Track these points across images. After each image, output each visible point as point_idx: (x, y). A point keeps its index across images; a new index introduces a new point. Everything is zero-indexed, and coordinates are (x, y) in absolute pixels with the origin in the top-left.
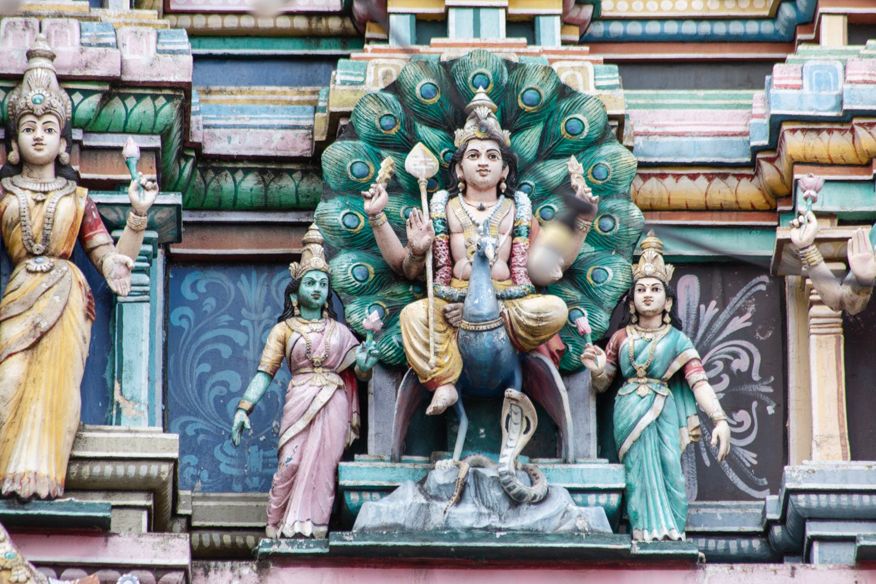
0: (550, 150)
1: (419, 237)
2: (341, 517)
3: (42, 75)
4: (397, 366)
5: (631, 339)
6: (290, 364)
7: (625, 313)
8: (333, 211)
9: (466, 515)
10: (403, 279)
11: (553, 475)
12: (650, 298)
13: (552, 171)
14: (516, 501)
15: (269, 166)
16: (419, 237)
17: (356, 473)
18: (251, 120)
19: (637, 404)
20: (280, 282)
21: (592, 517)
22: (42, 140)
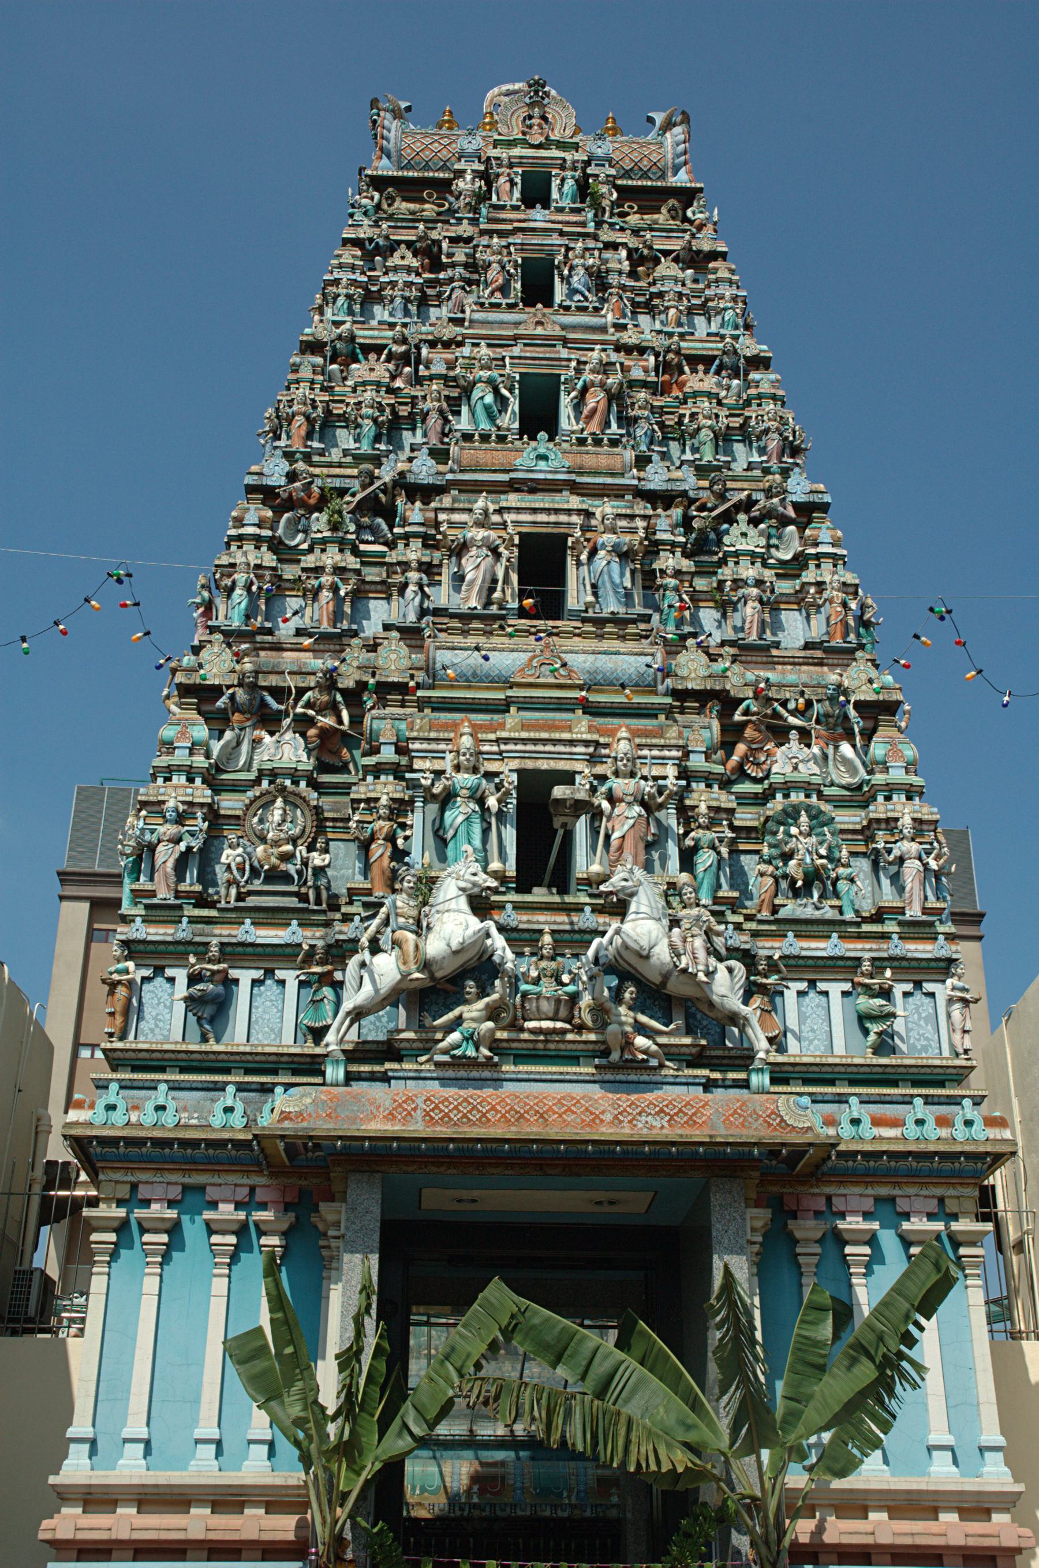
10: (787, 857)
11: (828, 903)
18: (746, 817)
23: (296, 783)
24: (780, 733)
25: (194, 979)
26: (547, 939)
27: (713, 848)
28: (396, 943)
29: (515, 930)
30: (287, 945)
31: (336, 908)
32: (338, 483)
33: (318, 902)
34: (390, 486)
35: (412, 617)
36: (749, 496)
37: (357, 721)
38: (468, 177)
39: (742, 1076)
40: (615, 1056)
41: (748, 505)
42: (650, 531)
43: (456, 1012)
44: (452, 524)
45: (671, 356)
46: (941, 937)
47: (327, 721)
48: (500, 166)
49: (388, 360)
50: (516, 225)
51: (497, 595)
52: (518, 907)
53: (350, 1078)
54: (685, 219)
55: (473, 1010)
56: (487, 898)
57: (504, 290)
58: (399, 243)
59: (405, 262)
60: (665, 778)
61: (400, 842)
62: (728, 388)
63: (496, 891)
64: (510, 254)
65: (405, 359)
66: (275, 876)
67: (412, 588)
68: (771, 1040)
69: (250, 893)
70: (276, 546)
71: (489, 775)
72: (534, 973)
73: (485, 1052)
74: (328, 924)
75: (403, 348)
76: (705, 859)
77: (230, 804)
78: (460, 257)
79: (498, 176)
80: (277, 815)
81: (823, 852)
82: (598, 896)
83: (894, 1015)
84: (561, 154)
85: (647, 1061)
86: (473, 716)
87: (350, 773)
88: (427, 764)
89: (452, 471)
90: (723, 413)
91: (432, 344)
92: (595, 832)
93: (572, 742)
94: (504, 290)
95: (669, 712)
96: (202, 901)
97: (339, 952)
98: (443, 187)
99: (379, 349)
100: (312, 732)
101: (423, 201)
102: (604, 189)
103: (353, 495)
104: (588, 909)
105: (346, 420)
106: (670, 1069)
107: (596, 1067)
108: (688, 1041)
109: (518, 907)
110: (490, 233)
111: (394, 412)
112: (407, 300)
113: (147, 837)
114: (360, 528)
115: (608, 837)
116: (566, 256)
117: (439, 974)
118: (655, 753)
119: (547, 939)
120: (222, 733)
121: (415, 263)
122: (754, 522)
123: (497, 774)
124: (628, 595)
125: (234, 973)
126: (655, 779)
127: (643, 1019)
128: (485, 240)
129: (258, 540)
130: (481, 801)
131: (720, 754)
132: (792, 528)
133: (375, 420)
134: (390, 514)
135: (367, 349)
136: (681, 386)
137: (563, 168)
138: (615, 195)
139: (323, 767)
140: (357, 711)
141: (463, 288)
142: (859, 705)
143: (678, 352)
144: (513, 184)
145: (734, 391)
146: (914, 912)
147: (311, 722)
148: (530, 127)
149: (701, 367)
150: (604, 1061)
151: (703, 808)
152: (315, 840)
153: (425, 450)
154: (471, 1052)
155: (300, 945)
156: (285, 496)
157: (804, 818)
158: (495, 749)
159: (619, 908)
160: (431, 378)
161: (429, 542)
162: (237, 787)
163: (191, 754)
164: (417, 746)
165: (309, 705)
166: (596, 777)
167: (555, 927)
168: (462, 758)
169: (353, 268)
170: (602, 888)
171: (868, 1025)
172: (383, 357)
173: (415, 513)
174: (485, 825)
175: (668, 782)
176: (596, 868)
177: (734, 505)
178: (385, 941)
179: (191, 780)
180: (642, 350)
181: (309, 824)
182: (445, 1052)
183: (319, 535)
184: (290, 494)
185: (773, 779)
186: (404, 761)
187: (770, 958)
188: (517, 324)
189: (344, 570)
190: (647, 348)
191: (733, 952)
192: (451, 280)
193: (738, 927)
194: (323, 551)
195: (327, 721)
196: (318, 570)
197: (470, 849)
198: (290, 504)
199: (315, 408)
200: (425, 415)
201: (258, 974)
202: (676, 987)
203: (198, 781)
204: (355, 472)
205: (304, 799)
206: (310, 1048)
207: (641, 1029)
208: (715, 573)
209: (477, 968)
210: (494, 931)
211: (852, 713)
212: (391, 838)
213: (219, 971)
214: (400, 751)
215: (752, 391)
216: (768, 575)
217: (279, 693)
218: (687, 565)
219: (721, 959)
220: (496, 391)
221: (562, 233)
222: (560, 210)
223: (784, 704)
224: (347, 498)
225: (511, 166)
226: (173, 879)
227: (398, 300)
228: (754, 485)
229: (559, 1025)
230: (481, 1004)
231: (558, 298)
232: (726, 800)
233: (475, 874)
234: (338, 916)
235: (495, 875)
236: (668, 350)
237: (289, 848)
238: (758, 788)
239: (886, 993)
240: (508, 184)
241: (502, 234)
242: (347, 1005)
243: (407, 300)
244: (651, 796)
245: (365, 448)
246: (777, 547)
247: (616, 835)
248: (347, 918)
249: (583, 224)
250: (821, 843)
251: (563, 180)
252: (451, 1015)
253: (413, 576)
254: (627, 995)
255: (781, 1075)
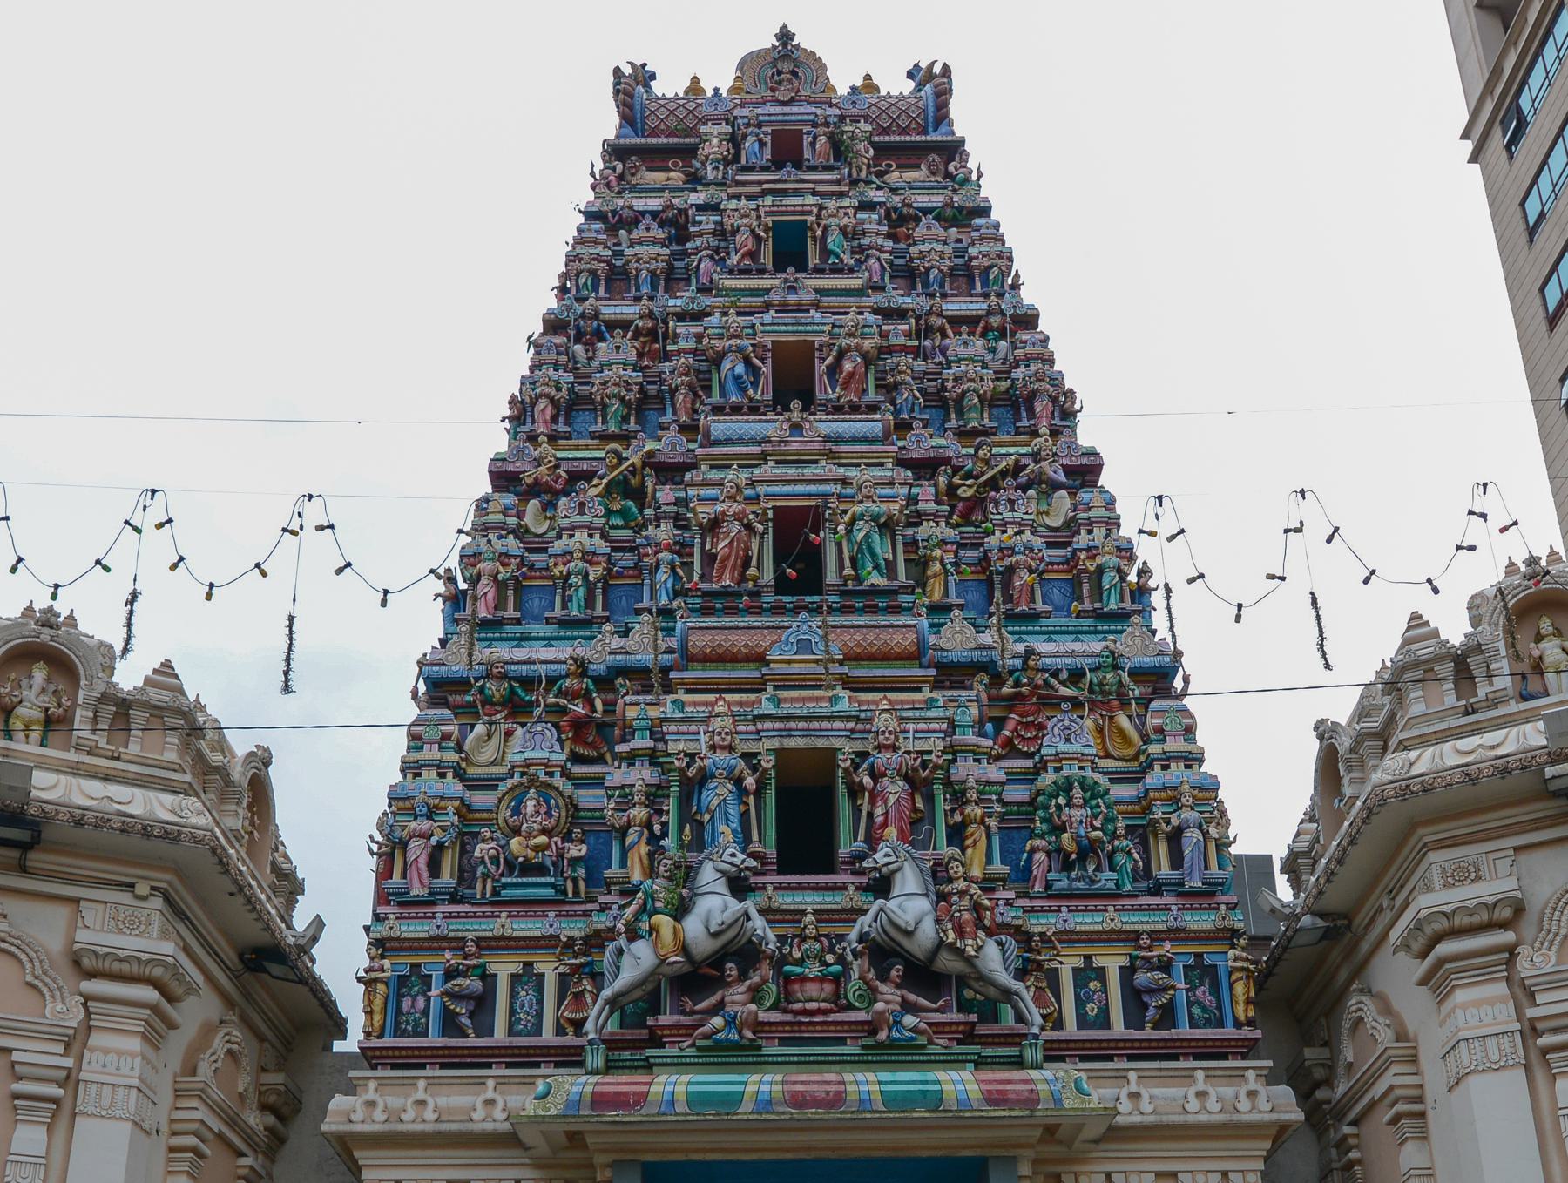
0: (1093, 797)
1: (1064, 818)
2: (1048, 886)
3: (971, 779)
4: (1059, 850)
5: (1117, 843)
6: (1033, 850)
7: (1114, 836)
8: (1041, 813)
9: (1081, 885)
12: (1121, 831)
13: (1094, 802)
14: (1093, 882)
15: (1019, 804)
16: (1064, 818)
17: (1052, 876)
18: (1017, 793)
19: (1120, 858)
20: (1024, 832)
21: (1111, 885)
22: (972, 795)
23: (551, 774)
24: (1051, 702)
25: (450, 974)
26: (810, 918)
27: (982, 822)
28: (653, 929)
29: (776, 911)
30: (544, 937)
31: (591, 899)
32: (585, 466)
33: (576, 893)
34: (639, 465)
35: (664, 600)
36: (1017, 461)
37: (609, 706)
38: (715, 141)
39: (1014, 1051)
40: (882, 1035)
41: (1018, 469)
42: (912, 500)
43: (718, 996)
44: (703, 501)
45: (933, 318)
46: (1223, 907)
47: (579, 709)
48: (748, 125)
49: (635, 337)
50: (765, 186)
51: (752, 571)
52: (779, 888)
53: (610, 1067)
54: (948, 175)
55: (736, 995)
56: (746, 879)
57: (753, 255)
58: (643, 213)
59: (651, 234)
60: (930, 752)
61: (657, 828)
62: (993, 350)
63: (757, 873)
64: (759, 217)
65: (652, 334)
66: (529, 868)
67: (663, 569)
68: (1044, 1017)
69: (505, 886)
70: (521, 533)
71: (747, 756)
72: (797, 955)
73: (748, 1034)
74: (587, 914)
75: (649, 324)
76: (976, 833)
77: (481, 799)
78: (708, 221)
79: (745, 136)
80: (530, 806)
81: (1097, 823)
82: (862, 872)
83: (1173, 987)
84: (814, 110)
85: (912, 1039)
86: (728, 697)
87: (606, 763)
88: (681, 746)
89: (701, 446)
90: (988, 374)
91: (681, 316)
92: (857, 811)
93: (831, 718)
94: (753, 255)
95: (937, 685)
96: (455, 899)
97: (597, 940)
98: (689, 152)
99: (625, 325)
100: (564, 721)
101: (668, 170)
102: (861, 147)
103: (601, 478)
104: (851, 888)
105: (593, 402)
106: (940, 1045)
107: (864, 1047)
108: (961, 1017)
109: (779, 888)
110: (737, 197)
111: (641, 391)
112: (653, 273)
113: (397, 834)
114: (609, 513)
115: (870, 815)
116: (819, 216)
117: (698, 958)
118: (922, 726)
119: (810, 918)
120: (472, 726)
121: (660, 234)
122: (1024, 488)
123: (755, 755)
124: (891, 567)
125: (492, 968)
126: (921, 753)
127: (912, 997)
128: (733, 204)
129: (503, 526)
130: (738, 782)
131: (989, 727)
132: (1064, 493)
133: (622, 399)
134: (639, 496)
135: (612, 325)
136: (943, 351)
137: (814, 124)
138: (872, 152)
139: (576, 758)
140: (611, 696)
141: (711, 257)
142: (1134, 673)
143: (940, 315)
144: (762, 144)
145: (1001, 355)
146: (1195, 883)
147: (563, 711)
148: (779, 83)
149: (964, 328)
150: (870, 1041)
151: (971, 782)
152: (570, 832)
153: (674, 427)
154: (734, 1036)
155: (558, 937)
156: (529, 481)
157: (1077, 788)
158: (751, 728)
159: (881, 886)
160: (679, 352)
161: (680, 522)
162: (488, 783)
163: (441, 748)
164: (673, 728)
165: (560, 694)
166: (858, 754)
167: (817, 907)
168: (717, 738)
169: (596, 242)
170: (865, 864)
171: (1146, 998)
172: (630, 334)
173: (665, 494)
174: (743, 808)
175: (933, 757)
176: (859, 845)
177: (1001, 472)
178: (645, 925)
179: (442, 775)
180: (901, 314)
181: (564, 814)
182: (706, 1037)
183: (566, 521)
184: (536, 479)
185: (1044, 751)
186: (661, 746)
187: (1042, 934)
188: (767, 291)
189: (594, 553)
190: (907, 311)
191: (1004, 927)
192: (698, 250)
193: (1008, 903)
194: (572, 536)
195: (579, 709)
196: (567, 555)
197: (728, 830)
198: (536, 489)
199: (559, 390)
200: (673, 391)
201: (517, 968)
202: (947, 962)
203: (450, 775)
204: (601, 454)
205: (557, 789)
206: (570, 1040)
207: (907, 1007)
208: (982, 544)
209: (738, 953)
210: (753, 912)
211: (1126, 679)
212: (648, 825)
213: (475, 967)
214: (657, 735)
215: (1018, 352)
216: (1038, 542)
217: (529, 683)
218: (951, 534)
219: (990, 933)
220: (747, 361)
221: (814, 193)
222: (813, 169)
223: (1055, 674)
224: (595, 481)
225: (760, 125)
226: (426, 874)
227: (644, 273)
228: (1023, 450)
229: (824, 1005)
230: (742, 988)
231: (813, 259)
232: (994, 772)
233: (733, 855)
234: (595, 907)
235: (753, 855)
236: (929, 313)
237: (543, 839)
238: (1029, 763)
239: (1166, 966)
240: (756, 145)
241: (750, 197)
242: (607, 993)
243: (653, 273)
244: (915, 769)
245: (613, 428)
246: (1047, 514)
247: (879, 811)
248: (605, 908)
249: (838, 182)
250: (1096, 817)
251: (815, 138)
252: (713, 1000)
253: (665, 556)
254: (894, 973)
255: (1056, 1053)
